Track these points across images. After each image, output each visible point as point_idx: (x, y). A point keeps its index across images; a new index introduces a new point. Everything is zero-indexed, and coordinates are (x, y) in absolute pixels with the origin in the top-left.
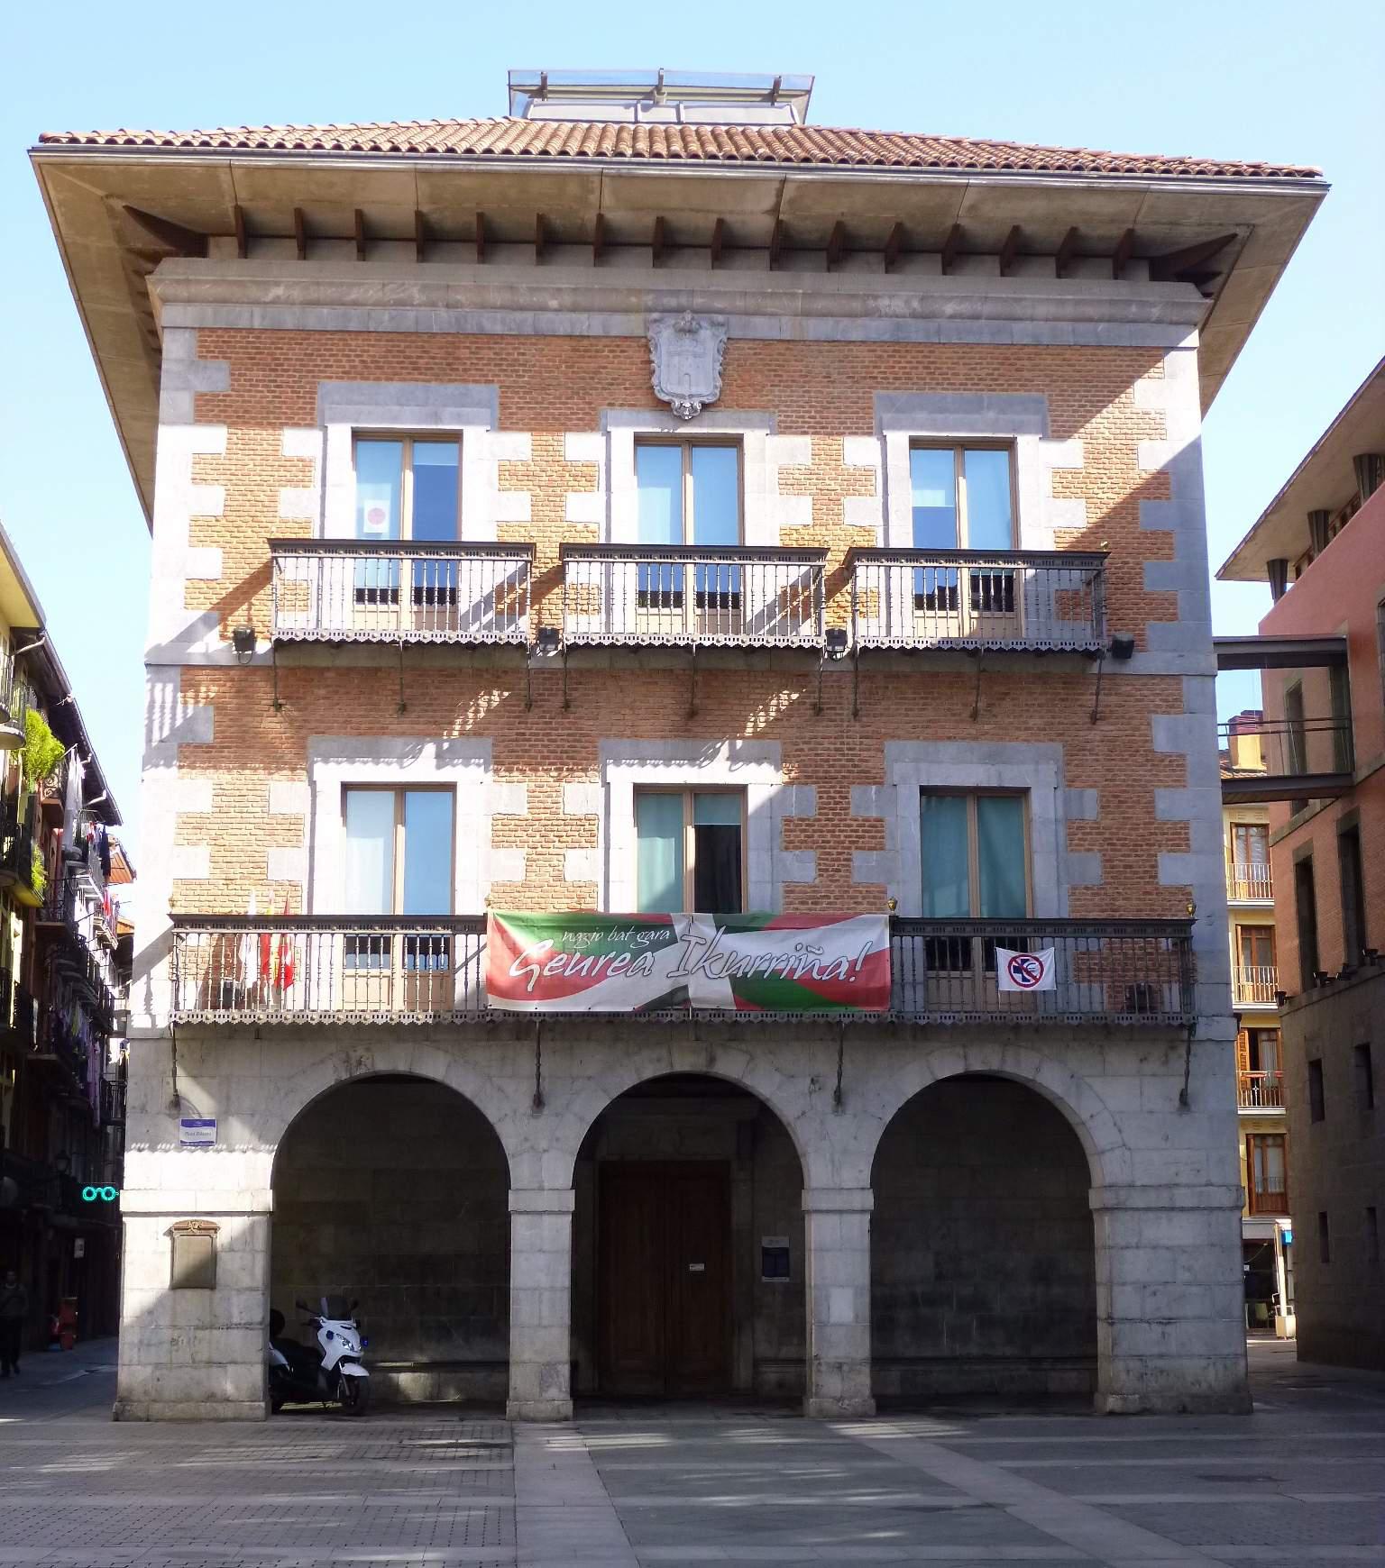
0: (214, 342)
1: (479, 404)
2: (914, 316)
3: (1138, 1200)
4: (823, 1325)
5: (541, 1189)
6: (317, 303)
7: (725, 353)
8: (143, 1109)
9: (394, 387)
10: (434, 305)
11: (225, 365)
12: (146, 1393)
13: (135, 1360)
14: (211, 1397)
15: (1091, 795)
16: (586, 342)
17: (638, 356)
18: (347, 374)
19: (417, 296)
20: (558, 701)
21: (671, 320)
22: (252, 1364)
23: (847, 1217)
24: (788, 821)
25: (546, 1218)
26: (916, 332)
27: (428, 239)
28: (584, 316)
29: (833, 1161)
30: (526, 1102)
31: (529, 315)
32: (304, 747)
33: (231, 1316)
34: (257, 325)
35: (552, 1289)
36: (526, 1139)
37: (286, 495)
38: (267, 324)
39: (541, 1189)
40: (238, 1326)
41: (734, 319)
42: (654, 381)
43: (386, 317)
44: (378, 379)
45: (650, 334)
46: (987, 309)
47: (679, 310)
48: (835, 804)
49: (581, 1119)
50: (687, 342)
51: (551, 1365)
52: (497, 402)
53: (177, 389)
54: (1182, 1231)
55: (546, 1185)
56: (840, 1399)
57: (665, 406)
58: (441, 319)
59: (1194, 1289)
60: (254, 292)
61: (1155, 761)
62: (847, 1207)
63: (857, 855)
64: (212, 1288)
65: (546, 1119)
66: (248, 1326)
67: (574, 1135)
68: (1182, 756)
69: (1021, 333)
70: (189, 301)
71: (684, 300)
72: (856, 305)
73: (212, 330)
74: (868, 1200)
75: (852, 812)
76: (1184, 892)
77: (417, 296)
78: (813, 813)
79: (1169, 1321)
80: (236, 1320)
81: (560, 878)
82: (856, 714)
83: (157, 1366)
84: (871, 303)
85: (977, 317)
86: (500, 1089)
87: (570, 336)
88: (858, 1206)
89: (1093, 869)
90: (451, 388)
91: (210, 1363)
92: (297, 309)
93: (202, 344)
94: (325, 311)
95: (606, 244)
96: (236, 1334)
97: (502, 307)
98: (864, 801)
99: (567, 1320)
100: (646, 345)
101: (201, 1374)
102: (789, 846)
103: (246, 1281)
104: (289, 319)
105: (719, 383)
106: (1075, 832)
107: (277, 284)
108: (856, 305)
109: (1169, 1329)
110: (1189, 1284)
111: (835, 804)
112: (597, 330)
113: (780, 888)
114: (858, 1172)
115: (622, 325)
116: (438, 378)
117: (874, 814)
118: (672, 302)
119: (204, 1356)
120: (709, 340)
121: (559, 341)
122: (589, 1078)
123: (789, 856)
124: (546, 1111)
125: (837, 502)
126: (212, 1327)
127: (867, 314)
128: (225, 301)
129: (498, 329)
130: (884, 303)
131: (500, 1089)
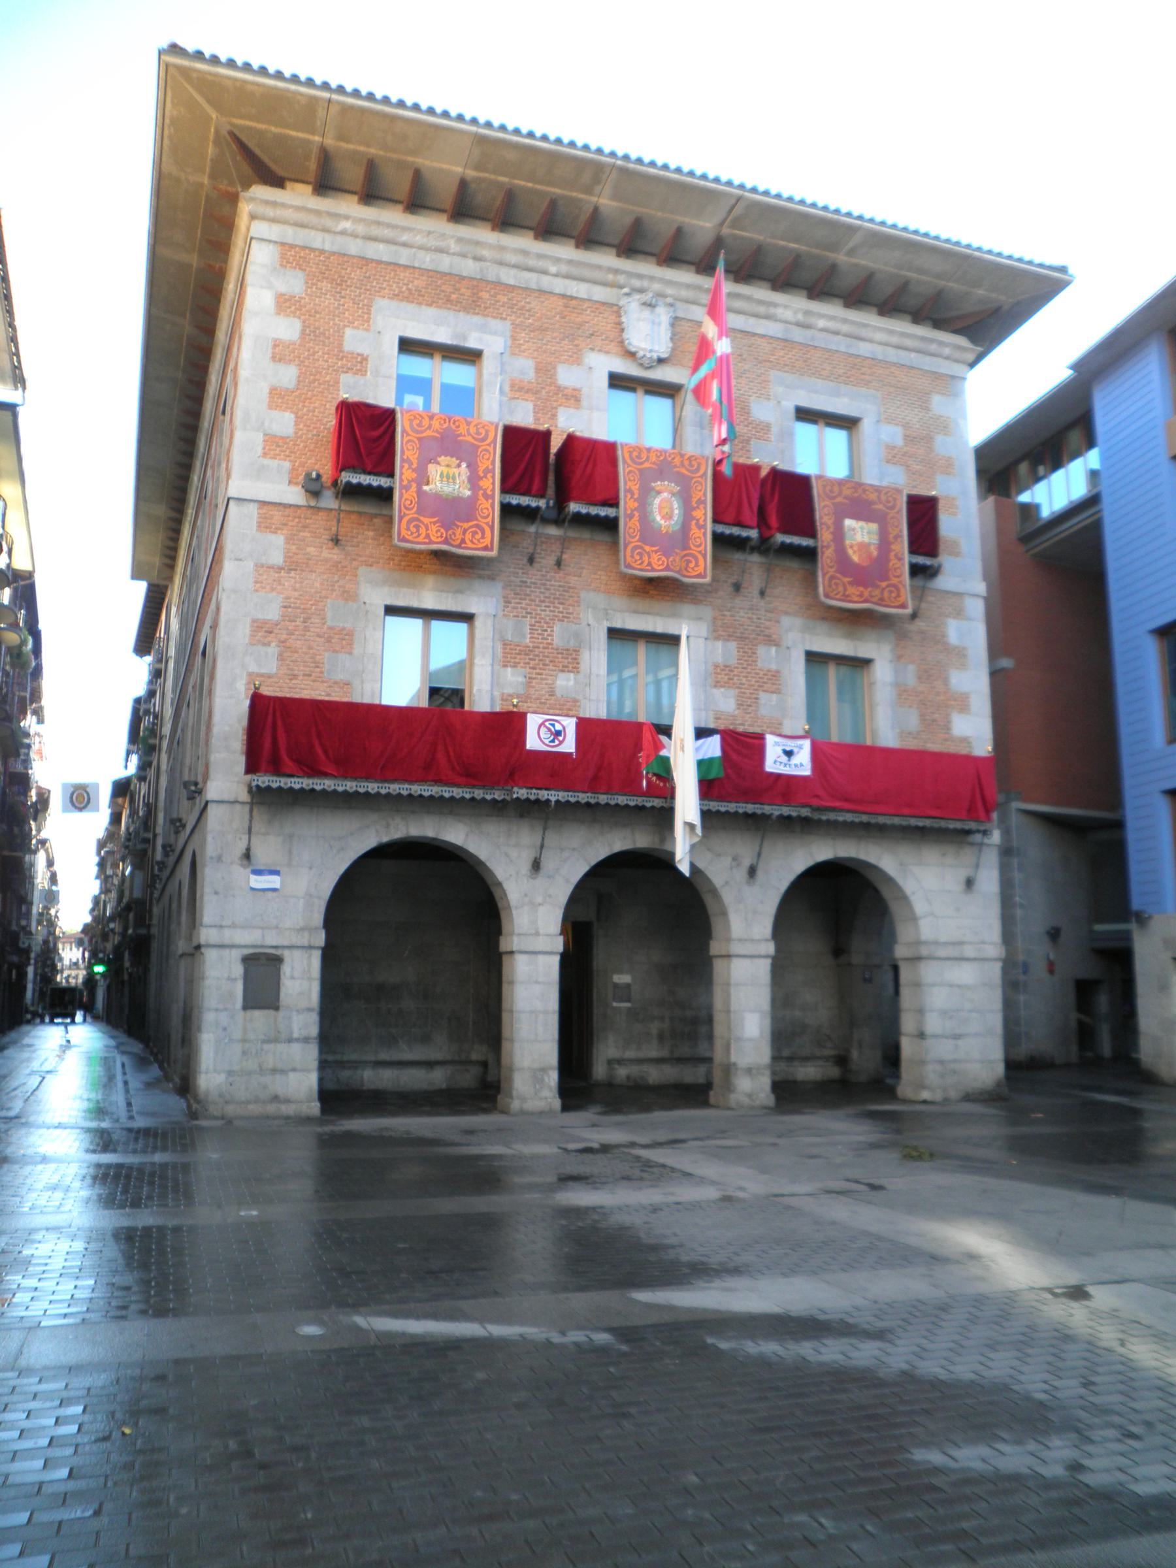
0: (292, 256)
1: (495, 333)
2: (798, 324)
3: (942, 953)
4: (739, 1039)
5: (537, 934)
6: (375, 239)
7: (673, 325)
8: (219, 859)
9: (431, 312)
10: (464, 256)
11: (300, 274)
12: (221, 1095)
13: (211, 1067)
14: (276, 1098)
15: (911, 668)
16: (574, 302)
17: (612, 318)
18: (395, 296)
19: (453, 246)
20: (552, 560)
21: (637, 296)
22: (309, 1071)
23: (757, 961)
24: (716, 666)
25: (541, 958)
26: (798, 335)
27: (463, 209)
28: (574, 283)
29: (746, 919)
30: (525, 866)
31: (533, 276)
32: (356, 576)
33: (292, 1033)
34: (327, 247)
35: (546, 1012)
36: (526, 895)
37: (345, 378)
38: (335, 249)
39: (537, 934)
40: (297, 1040)
41: (679, 304)
42: (625, 336)
43: (428, 259)
44: (420, 304)
45: (621, 303)
46: (845, 328)
47: (641, 291)
48: (748, 656)
49: (567, 881)
50: (647, 313)
51: (544, 1070)
52: (508, 334)
53: (262, 287)
54: (965, 974)
55: (541, 931)
56: (750, 1096)
57: (631, 355)
58: (468, 267)
59: (974, 1015)
60: (328, 222)
61: (947, 648)
62: (756, 953)
63: (764, 697)
64: (277, 1008)
65: (540, 881)
66: (306, 1040)
67: (562, 892)
68: (964, 648)
69: (864, 349)
70: (274, 220)
71: (645, 283)
72: (762, 310)
73: (292, 246)
74: (770, 948)
75: (760, 664)
76: (965, 740)
77: (453, 246)
78: (733, 662)
79: (957, 1037)
80: (296, 1035)
81: (552, 693)
82: (762, 593)
83: (230, 1073)
84: (772, 310)
85: (836, 333)
86: (506, 855)
87: (563, 296)
88: (763, 952)
89: (913, 720)
90: (476, 319)
91: (274, 1071)
92: (359, 241)
93: (283, 256)
94: (381, 246)
95: (589, 236)
96: (296, 1047)
97: (516, 266)
98: (767, 657)
99: (556, 1036)
100: (617, 310)
101: (267, 1079)
102: (717, 684)
103: (303, 1004)
104: (354, 247)
105: (671, 345)
106: (903, 694)
107: (347, 218)
108: (762, 310)
109: (960, 1042)
110: (971, 1011)
111: (748, 656)
112: (583, 295)
113: (711, 714)
114: (763, 927)
115: (600, 293)
116: (466, 310)
117: (774, 667)
118: (637, 283)
119: (270, 1062)
120: (663, 315)
121: (555, 298)
122: (574, 849)
123: (718, 693)
124: (543, 872)
125: (748, 441)
126: (276, 1040)
127: (767, 317)
128: (302, 225)
129: (511, 282)
130: (779, 312)
131: (506, 855)
